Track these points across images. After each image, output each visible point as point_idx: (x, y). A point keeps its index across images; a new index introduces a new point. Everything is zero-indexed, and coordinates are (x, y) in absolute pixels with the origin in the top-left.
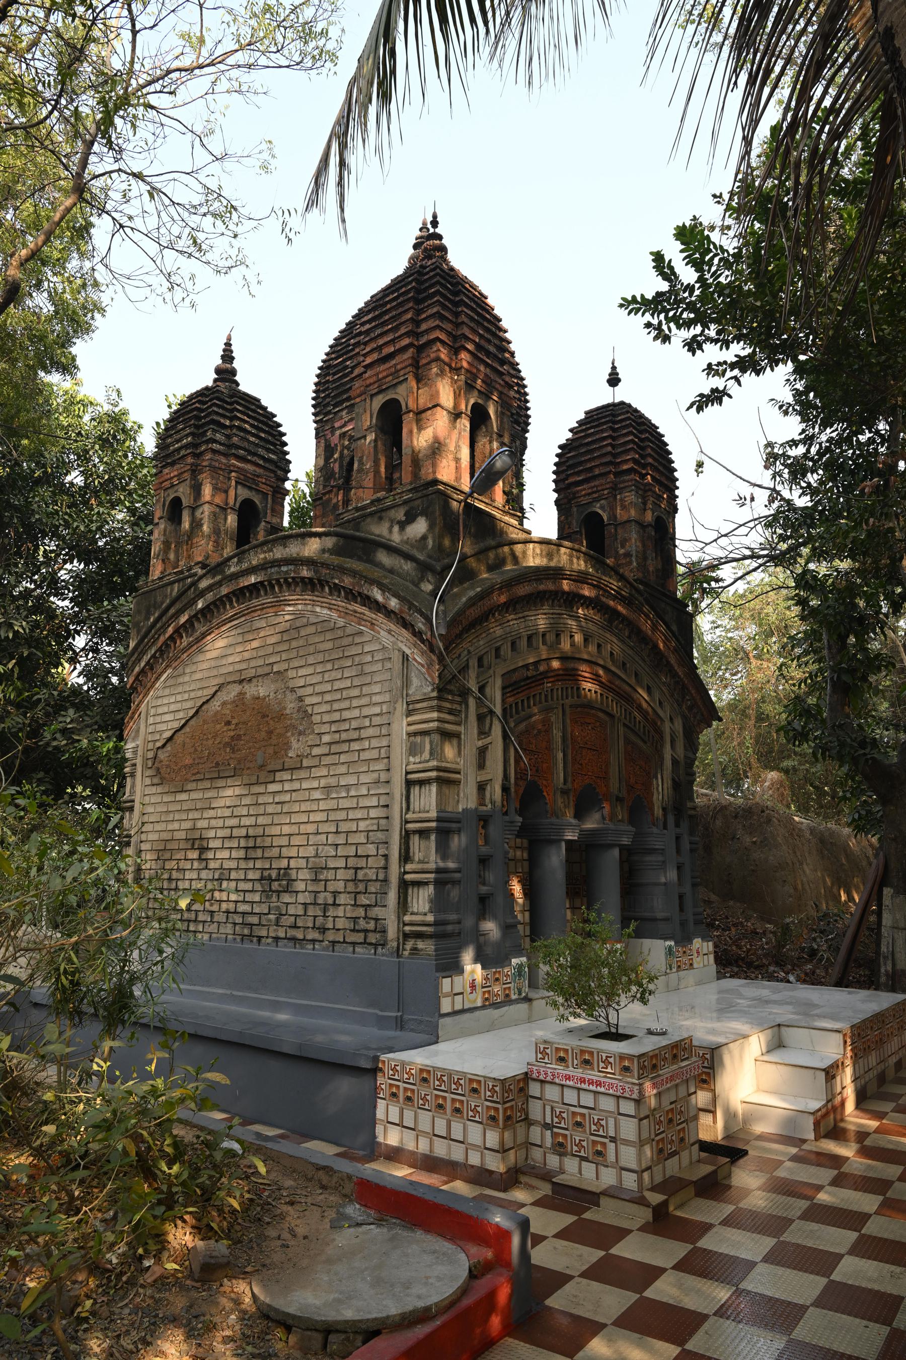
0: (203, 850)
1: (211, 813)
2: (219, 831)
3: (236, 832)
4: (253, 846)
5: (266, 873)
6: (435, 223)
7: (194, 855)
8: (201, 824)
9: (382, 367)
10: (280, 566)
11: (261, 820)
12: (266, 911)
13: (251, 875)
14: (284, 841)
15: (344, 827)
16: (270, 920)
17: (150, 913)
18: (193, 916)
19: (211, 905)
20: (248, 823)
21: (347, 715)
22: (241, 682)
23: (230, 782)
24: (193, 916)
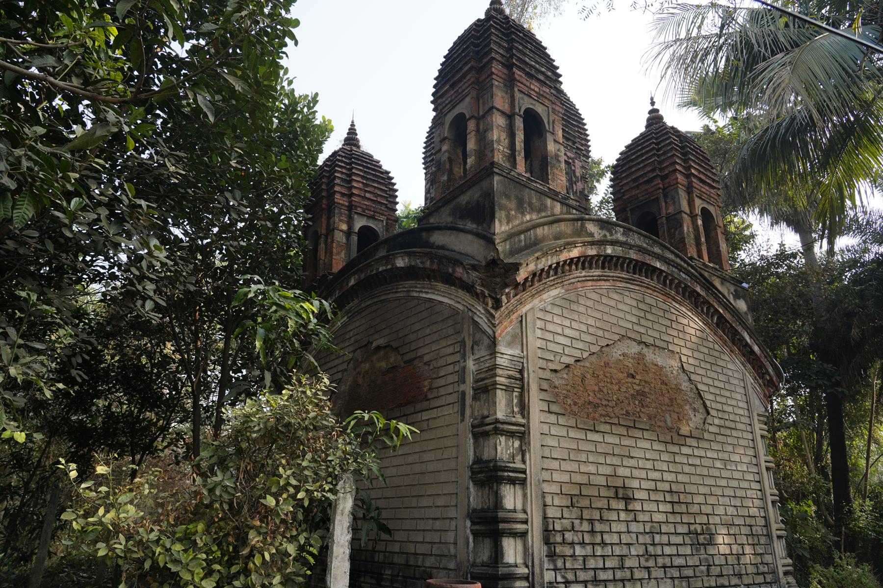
0: (628, 500)
1: (632, 462)
2: (642, 482)
3: (660, 486)
4: (677, 500)
5: (692, 528)
6: (653, 103)
7: (621, 505)
8: (621, 472)
9: (707, 188)
10: (680, 271)
11: (680, 478)
12: (698, 563)
13: (681, 529)
14: (699, 499)
15: (739, 493)
16: (702, 572)
17: (570, 576)
18: (628, 574)
19: (647, 560)
20: (670, 479)
21: (726, 408)
22: (640, 343)
23: (647, 435)
24: (628, 574)
